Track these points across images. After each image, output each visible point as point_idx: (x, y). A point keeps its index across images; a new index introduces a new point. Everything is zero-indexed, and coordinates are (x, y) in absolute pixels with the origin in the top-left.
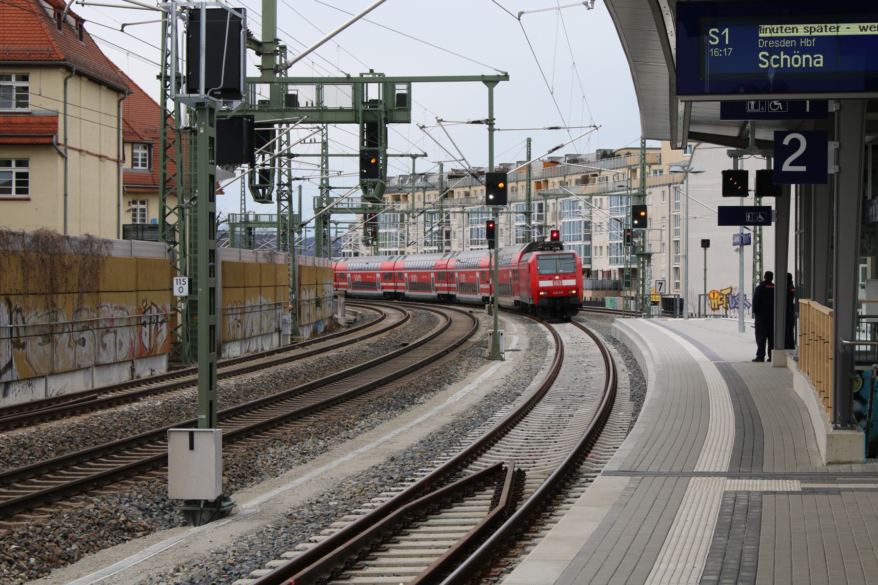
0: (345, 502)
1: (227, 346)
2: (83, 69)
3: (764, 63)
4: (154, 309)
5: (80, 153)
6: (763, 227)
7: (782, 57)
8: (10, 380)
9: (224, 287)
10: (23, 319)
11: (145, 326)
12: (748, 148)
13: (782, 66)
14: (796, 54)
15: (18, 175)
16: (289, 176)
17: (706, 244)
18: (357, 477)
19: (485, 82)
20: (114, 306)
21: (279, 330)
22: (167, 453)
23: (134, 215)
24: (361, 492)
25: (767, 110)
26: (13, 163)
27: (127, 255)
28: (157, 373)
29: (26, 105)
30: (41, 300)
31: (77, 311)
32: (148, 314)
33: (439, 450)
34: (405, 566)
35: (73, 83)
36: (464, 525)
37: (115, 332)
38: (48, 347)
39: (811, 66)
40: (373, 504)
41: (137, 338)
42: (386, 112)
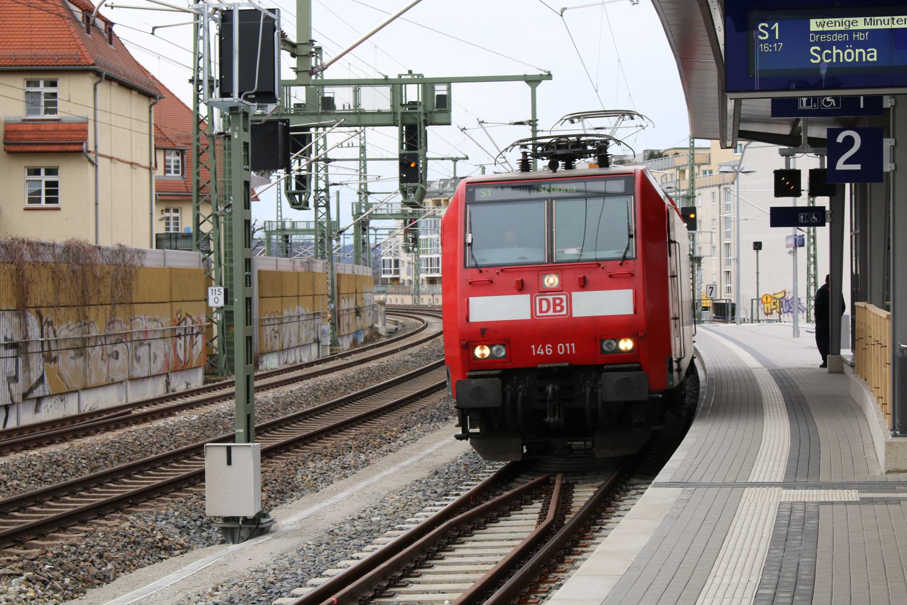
0: (388, 518)
1: (265, 358)
2: (113, 74)
3: (816, 58)
4: (189, 321)
5: (111, 162)
6: (818, 228)
7: (835, 51)
8: (41, 394)
9: (261, 297)
10: (55, 332)
11: (180, 338)
12: (800, 146)
13: (834, 61)
14: (849, 48)
15: (48, 184)
16: (327, 181)
17: (758, 246)
18: (400, 492)
19: (527, 82)
20: (147, 317)
21: (317, 341)
22: (204, 469)
23: (168, 224)
24: (404, 507)
25: (820, 107)
26: (43, 172)
27: (161, 264)
28: (193, 387)
29: (54, 112)
30: (73, 312)
31: (109, 324)
32: (183, 325)
33: (484, 463)
34: (450, 583)
35: (104, 89)
36: (511, 540)
37: (149, 345)
38: (80, 361)
39: (864, 60)
40: (419, 519)
41: (172, 351)
42: (425, 114)
